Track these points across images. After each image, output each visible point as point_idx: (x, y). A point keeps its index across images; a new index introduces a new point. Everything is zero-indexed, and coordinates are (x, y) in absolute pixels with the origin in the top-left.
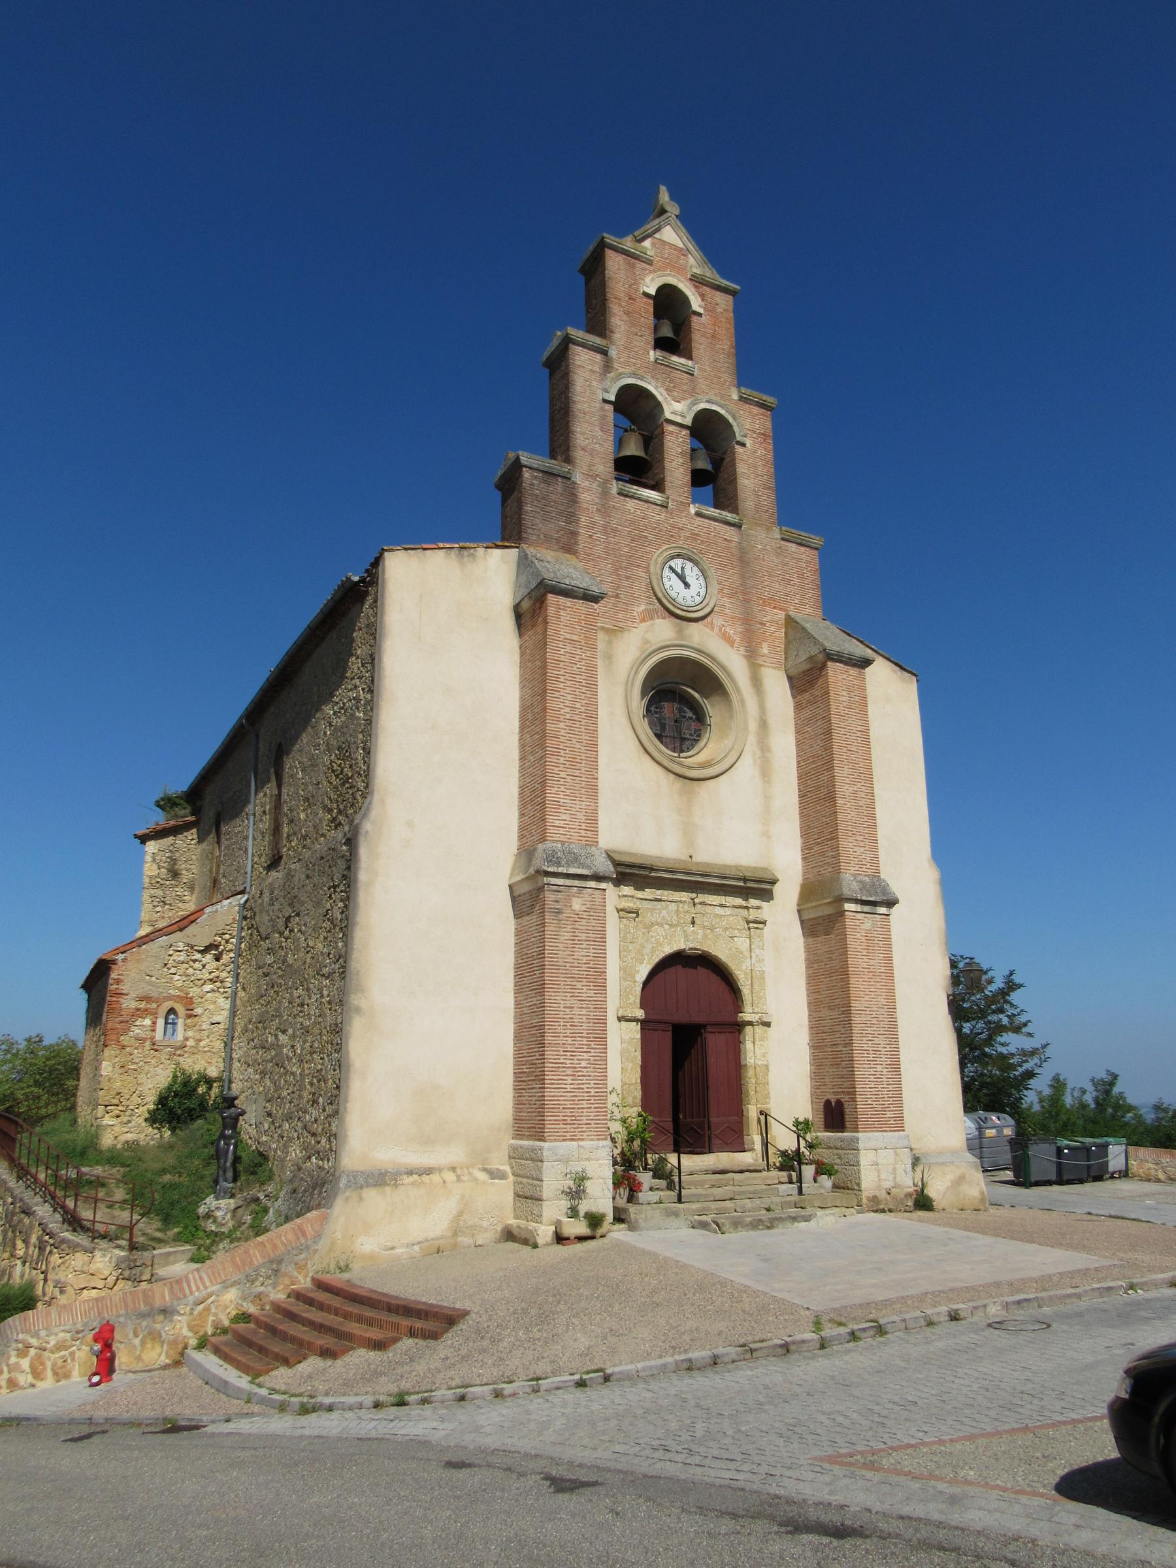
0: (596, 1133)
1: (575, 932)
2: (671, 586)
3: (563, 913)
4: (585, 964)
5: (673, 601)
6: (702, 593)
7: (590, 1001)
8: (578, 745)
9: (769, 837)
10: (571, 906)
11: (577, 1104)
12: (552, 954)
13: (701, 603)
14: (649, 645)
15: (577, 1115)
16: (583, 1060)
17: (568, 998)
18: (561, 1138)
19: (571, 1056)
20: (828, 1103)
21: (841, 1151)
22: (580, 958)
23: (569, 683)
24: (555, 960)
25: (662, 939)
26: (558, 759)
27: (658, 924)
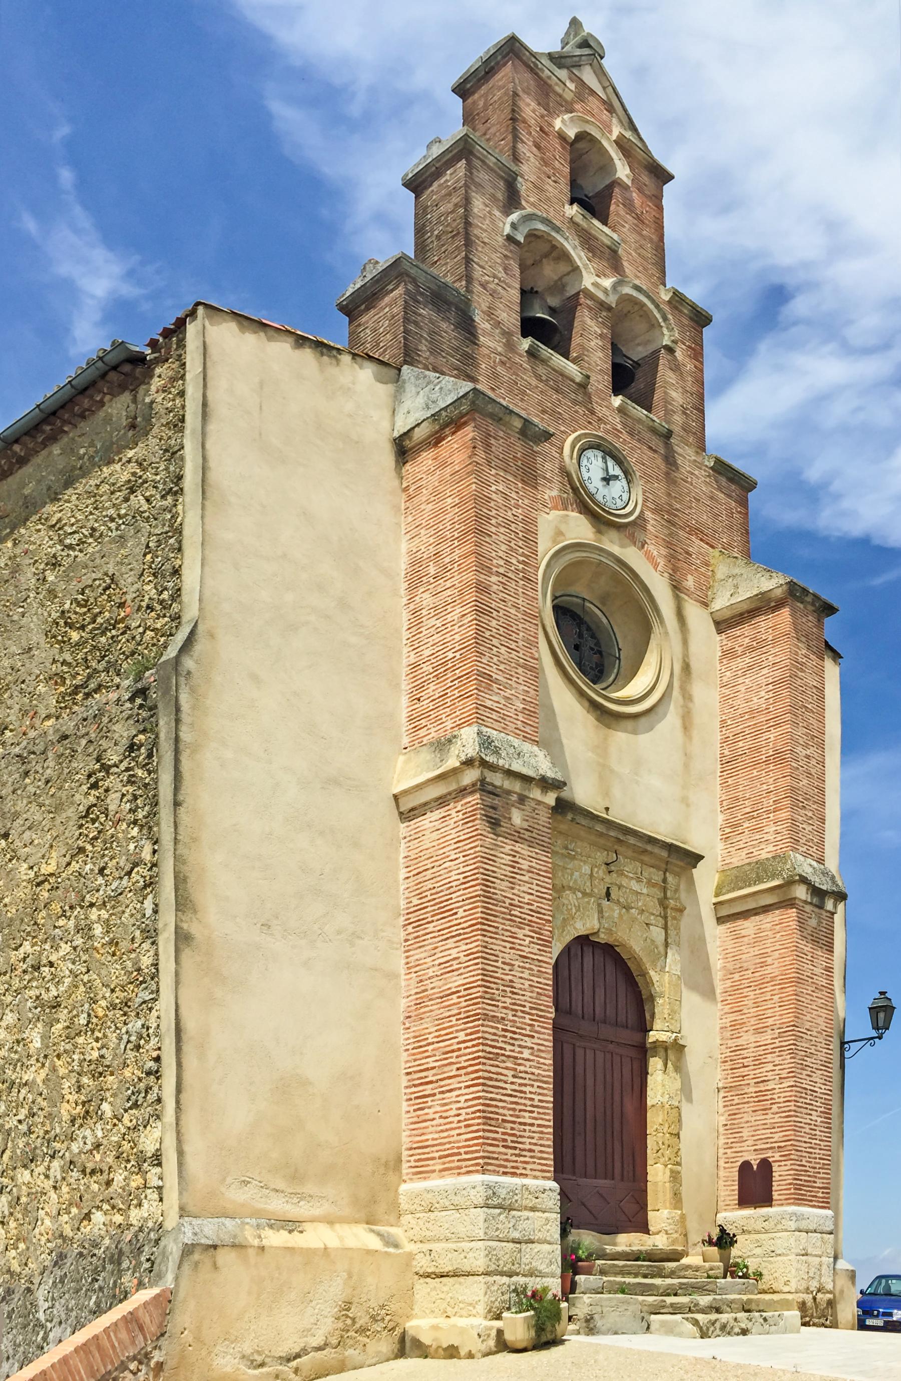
0: (540, 1167)
1: (515, 856)
2: (589, 478)
3: (500, 826)
4: (528, 904)
5: (591, 496)
6: (625, 497)
7: (533, 959)
8: (513, 611)
9: (688, 805)
10: (510, 819)
11: (518, 1117)
12: (488, 881)
13: (624, 508)
14: (563, 538)
15: (518, 1133)
16: (525, 1047)
17: (507, 950)
18: (502, 1170)
19: (512, 1038)
20: (745, 1167)
21: (763, 1236)
22: (522, 895)
23: (502, 530)
24: (492, 890)
25: (574, 911)
26: (489, 621)
27: (570, 888)
